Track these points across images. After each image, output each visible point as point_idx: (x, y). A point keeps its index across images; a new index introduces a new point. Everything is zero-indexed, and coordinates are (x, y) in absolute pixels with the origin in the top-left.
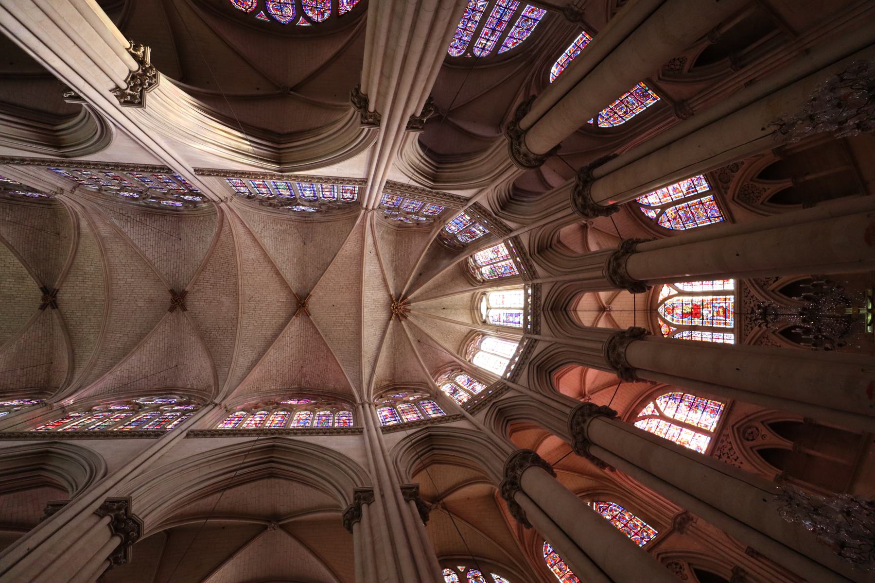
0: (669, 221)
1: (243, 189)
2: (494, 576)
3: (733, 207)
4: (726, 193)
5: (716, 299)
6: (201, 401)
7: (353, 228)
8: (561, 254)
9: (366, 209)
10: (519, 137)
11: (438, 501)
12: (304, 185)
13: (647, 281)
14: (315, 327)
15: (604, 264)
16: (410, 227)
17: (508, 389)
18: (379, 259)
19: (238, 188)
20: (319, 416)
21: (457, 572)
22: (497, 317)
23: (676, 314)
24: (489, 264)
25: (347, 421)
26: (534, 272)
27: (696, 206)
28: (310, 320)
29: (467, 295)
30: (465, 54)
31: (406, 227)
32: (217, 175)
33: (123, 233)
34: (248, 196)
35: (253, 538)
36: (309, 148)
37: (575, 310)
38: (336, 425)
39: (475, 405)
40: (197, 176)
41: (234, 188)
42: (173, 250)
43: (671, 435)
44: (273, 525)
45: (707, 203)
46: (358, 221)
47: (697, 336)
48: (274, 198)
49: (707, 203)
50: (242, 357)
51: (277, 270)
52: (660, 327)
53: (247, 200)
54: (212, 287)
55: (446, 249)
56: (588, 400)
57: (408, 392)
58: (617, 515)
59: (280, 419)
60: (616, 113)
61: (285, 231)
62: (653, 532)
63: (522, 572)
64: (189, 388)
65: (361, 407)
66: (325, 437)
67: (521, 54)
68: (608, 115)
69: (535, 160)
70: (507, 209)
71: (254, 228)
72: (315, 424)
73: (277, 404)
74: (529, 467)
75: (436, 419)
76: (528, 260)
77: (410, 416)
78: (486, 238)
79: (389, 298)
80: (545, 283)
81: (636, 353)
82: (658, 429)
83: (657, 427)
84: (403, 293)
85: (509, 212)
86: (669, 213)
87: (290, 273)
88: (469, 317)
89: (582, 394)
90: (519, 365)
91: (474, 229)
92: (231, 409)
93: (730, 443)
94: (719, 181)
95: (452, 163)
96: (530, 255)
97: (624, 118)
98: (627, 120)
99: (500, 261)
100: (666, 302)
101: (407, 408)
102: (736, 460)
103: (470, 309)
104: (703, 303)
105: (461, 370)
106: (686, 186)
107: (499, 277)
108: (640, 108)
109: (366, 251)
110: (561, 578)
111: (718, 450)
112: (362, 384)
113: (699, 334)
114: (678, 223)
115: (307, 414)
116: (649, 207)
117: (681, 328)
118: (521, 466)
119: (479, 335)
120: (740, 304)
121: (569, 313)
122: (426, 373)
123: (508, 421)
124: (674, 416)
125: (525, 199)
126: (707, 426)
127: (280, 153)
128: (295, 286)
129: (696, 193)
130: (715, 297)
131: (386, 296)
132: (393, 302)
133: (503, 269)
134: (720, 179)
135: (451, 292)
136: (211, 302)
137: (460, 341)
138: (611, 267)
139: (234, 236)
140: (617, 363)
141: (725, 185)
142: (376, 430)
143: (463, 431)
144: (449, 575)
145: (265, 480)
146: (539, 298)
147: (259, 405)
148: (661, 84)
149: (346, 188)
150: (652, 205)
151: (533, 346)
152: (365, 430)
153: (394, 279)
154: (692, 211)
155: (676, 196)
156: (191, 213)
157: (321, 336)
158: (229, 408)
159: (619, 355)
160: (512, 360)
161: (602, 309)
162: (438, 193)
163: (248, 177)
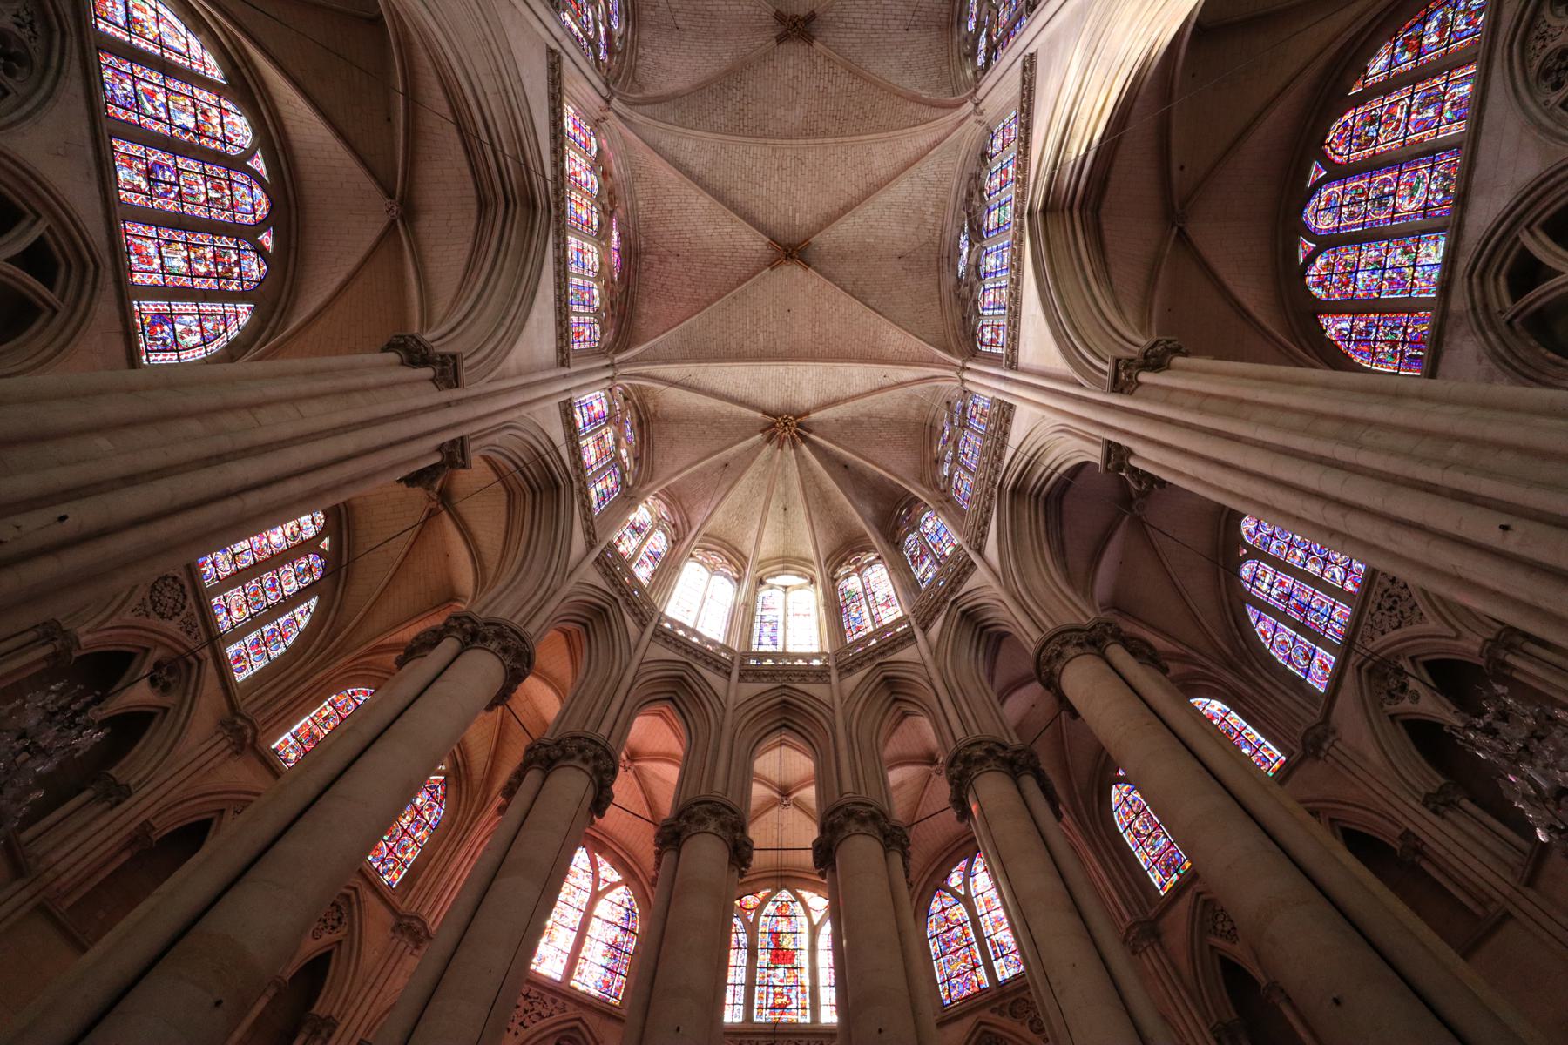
0: (943, 910)
1: (998, 143)
2: (313, 602)
3: (969, 1022)
4: (993, 1011)
5: (803, 992)
6: (615, 75)
7: (930, 344)
8: (883, 719)
9: (964, 368)
10: (1093, 643)
11: (442, 503)
12: (1005, 254)
13: (834, 871)
14: (750, 278)
15: (864, 794)
16: (931, 447)
17: (643, 625)
18: (873, 392)
19: (1000, 135)
20: (590, 289)
21: (319, 537)
22: (771, 605)
23: (777, 922)
24: (864, 589)
25: (581, 339)
26: (850, 671)
27: (970, 959)
28: (763, 269)
29: (810, 552)
30: (1246, 546)
31: (931, 441)
32: (1023, 95)
34: (986, 153)
35: (372, 172)
36: (1073, 264)
37: (781, 744)
38: (574, 319)
39: (613, 566)
40: (1021, 58)
41: (1001, 126)
42: (886, 17)
43: (564, 912)
44: (395, 208)
45: (974, 978)
46: (940, 353)
47: (737, 958)
48: (982, 200)
49: (974, 978)
50: (695, 146)
51: (852, 209)
52: (754, 893)
53: (979, 152)
54: (821, 89)
55: (893, 512)
56: (624, 767)
57: (636, 447)
58: (422, 816)
59: (585, 217)
60: (1137, 816)
61: (924, 221)
62: (394, 879)
63: (321, 652)
64: (637, 52)
65: (607, 362)
66: (553, 300)
67: (1244, 646)
68: (1134, 801)
69: (1051, 673)
70: (962, 623)
71: (928, 164)
72: (575, 281)
73: (612, 212)
74: (503, 664)
75: (588, 496)
76: (872, 659)
77: (592, 450)
78: (912, 585)
79: (803, 411)
80: (831, 691)
81: (706, 851)
82: (573, 889)
83: (578, 888)
84: (812, 436)
85: (958, 627)
86: (958, 909)
87: (846, 230)
88: (771, 555)
89: (633, 756)
90: (685, 644)
91: (928, 562)
92: (601, 129)
93: (551, 1015)
94: (1013, 998)
95: (1046, 522)
96: (880, 664)
97: (1129, 830)
98: (1125, 836)
99: (870, 609)
100: (798, 903)
101: (607, 446)
102: (521, 1024)
103: (783, 557)
104: (797, 968)
105: (675, 542)
106: (1005, 941)
107: (842, 608)
108: (1146, 860)
109: (888, 369)
110: (312, 719)
111: (539, 993)
112: (648, 364)
113: (743, 961)
114: (939, 926)
115: (593, 266)
116: (968, 874)
117: (752, 929)
118: (505, 650)
119: (739, 572)
120: (795, 1034)
121: (777, 733)
122: (669, 478)
123: (585, 625)
124: (597, 917)
125: (981, 655)
126: (580, 974)
127: (1063, 211)
128: (824, 240)
129: (993, 958)
130: (807, 989)
131: (807, 405)
132: (796, 418)
133: (857, 615)
134: (1017, 1000)
135: (815, 523)
136: (793, 88)
137: (727, 538)
138: (859, 808)
139: (914, 129)
140: (688, 819)
141: (1006, 1010)
142: (567, 391)
143: (565, 544)
144: (313, 523)
145: (473, 192)
146: (803, 679)
147: (609, 179)
148: (1188, 897)
149: (1001, 332)
150: (971, 879)
151: (718, 668)
152: (565, 371)
153: (837, 420)
154: (961, 951)
155: (988, 923)
156: (956, 49)
157: (734, 289)
158: (603, 125)
159: (702, 821)
160: (695, 632)
161: (785, 792)
162: (991, 497)
163: (1019, 153)
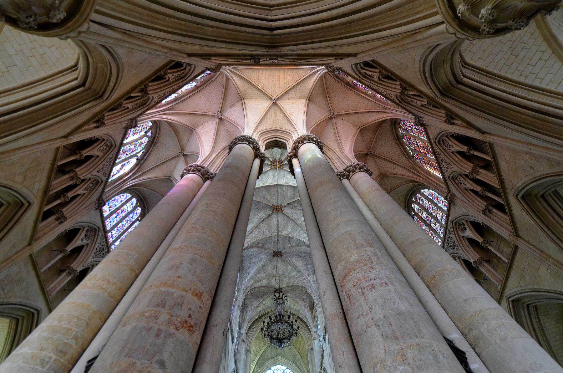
2: (422, 191)
33: (251, 276)
128: (268, 212)
131: (271, 170)
